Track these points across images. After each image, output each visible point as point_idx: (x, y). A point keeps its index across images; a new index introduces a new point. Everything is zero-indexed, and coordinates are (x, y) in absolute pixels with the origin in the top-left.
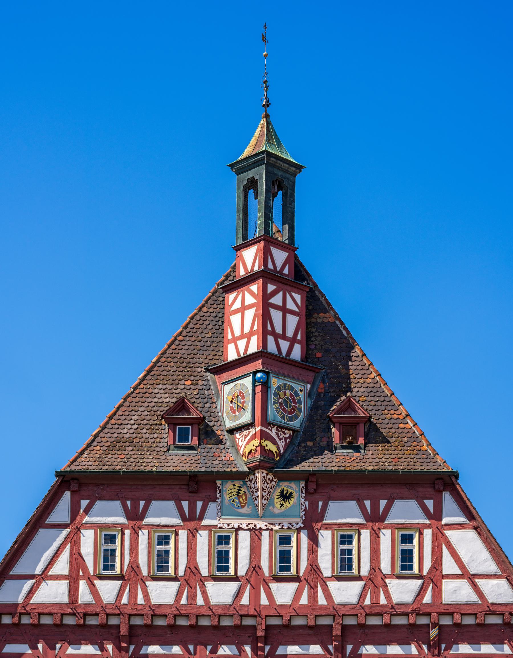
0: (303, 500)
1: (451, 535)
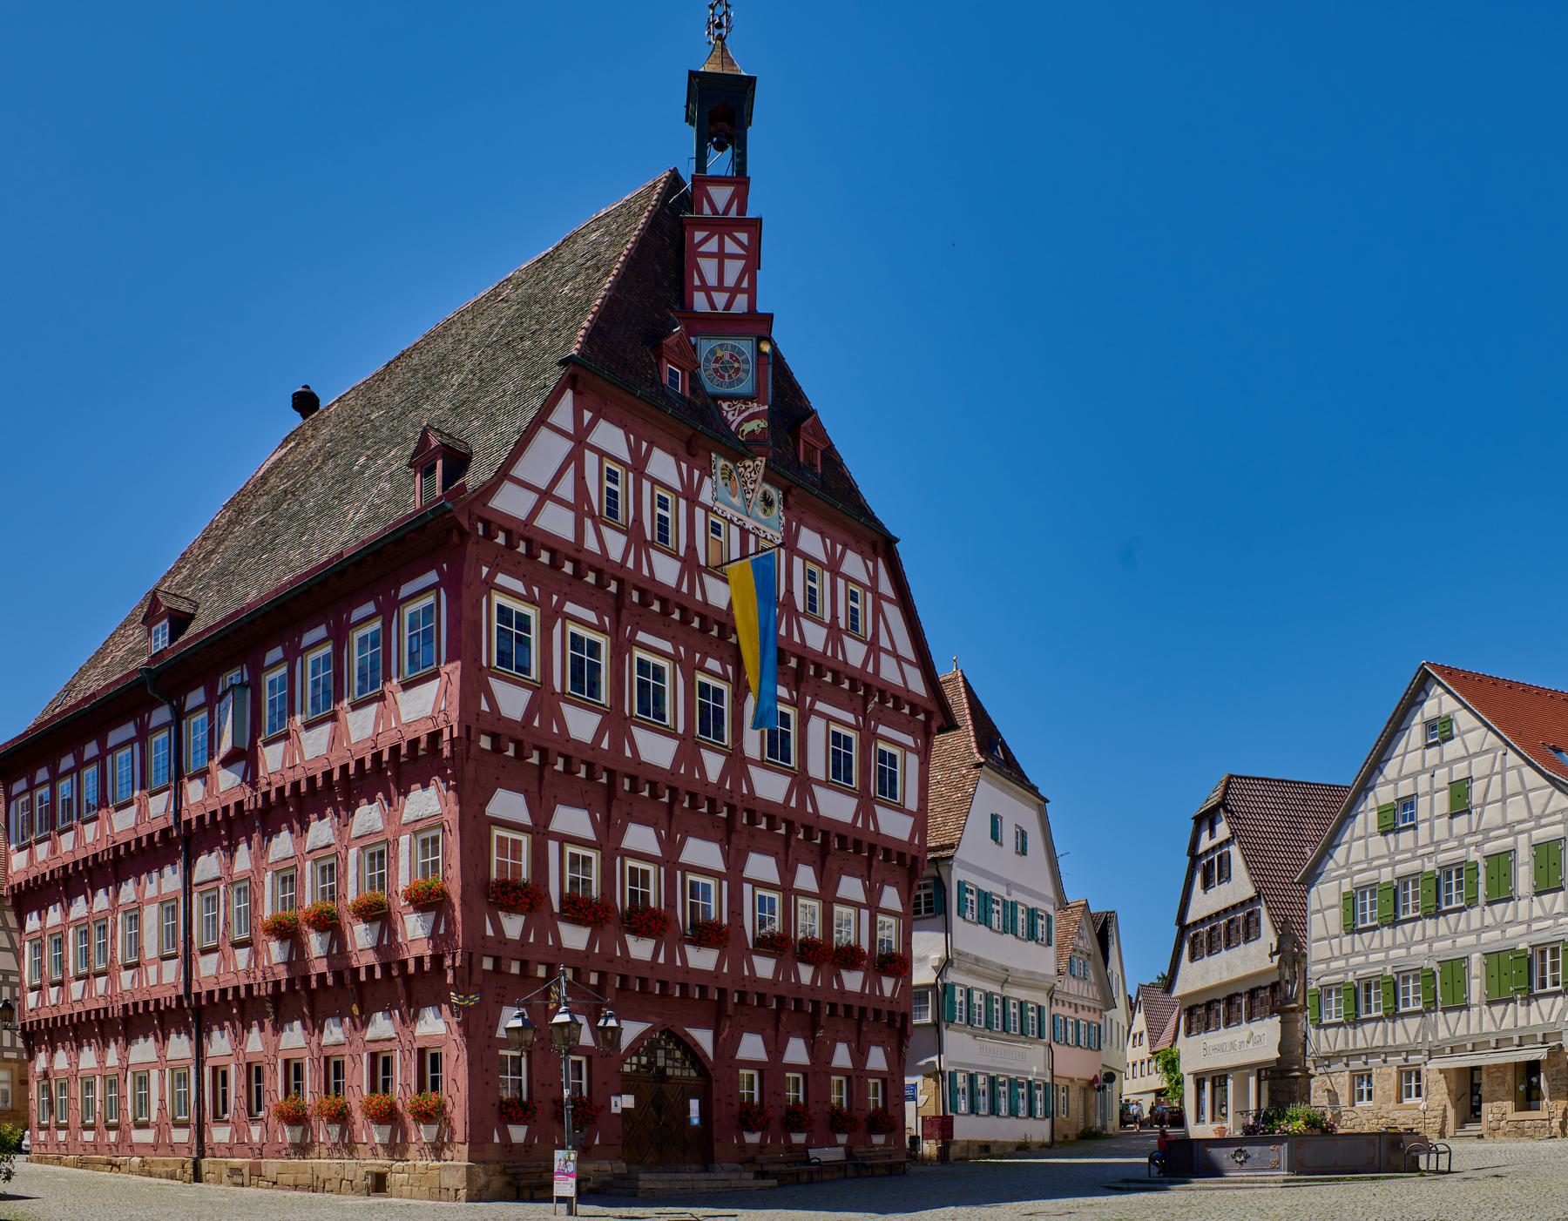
1: (885, 604)
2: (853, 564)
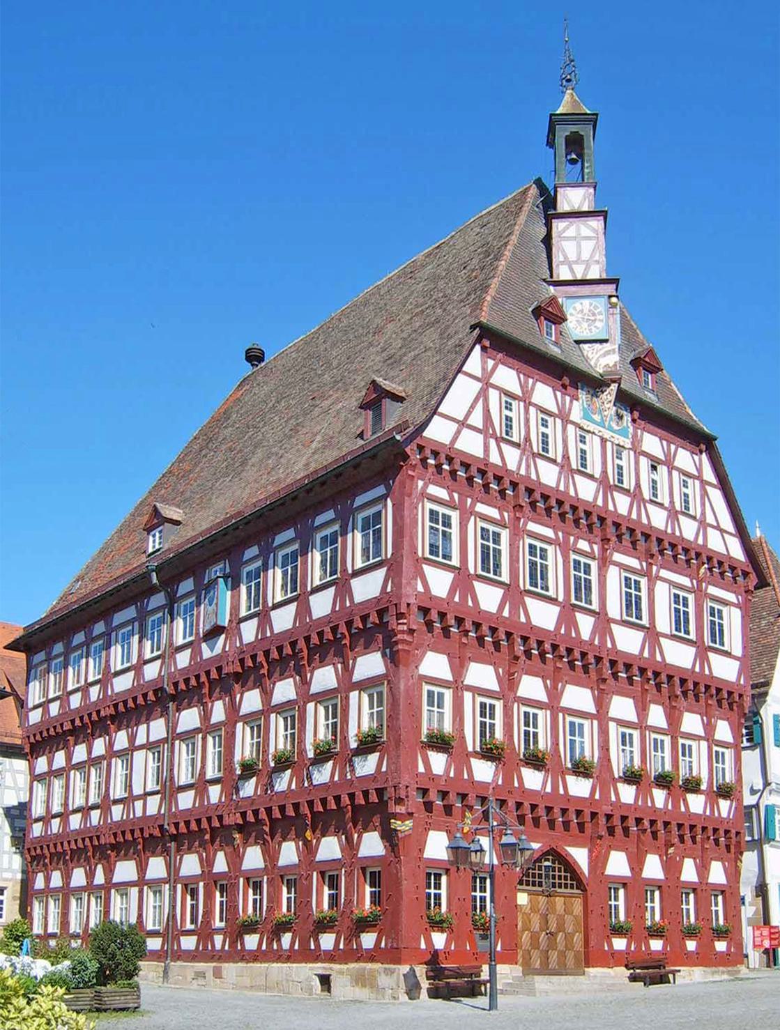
0: (629, 424)
1: (709, 488)
2: (684, 459)
